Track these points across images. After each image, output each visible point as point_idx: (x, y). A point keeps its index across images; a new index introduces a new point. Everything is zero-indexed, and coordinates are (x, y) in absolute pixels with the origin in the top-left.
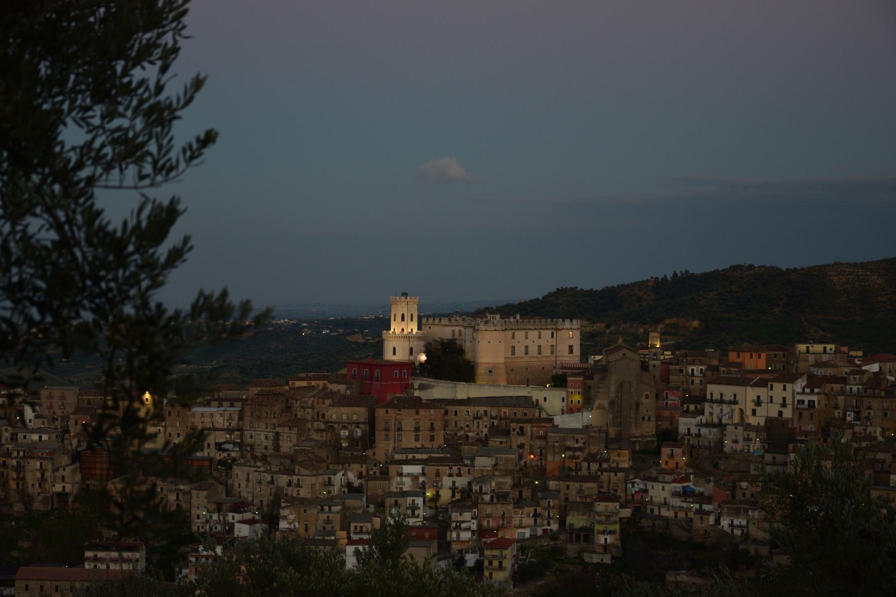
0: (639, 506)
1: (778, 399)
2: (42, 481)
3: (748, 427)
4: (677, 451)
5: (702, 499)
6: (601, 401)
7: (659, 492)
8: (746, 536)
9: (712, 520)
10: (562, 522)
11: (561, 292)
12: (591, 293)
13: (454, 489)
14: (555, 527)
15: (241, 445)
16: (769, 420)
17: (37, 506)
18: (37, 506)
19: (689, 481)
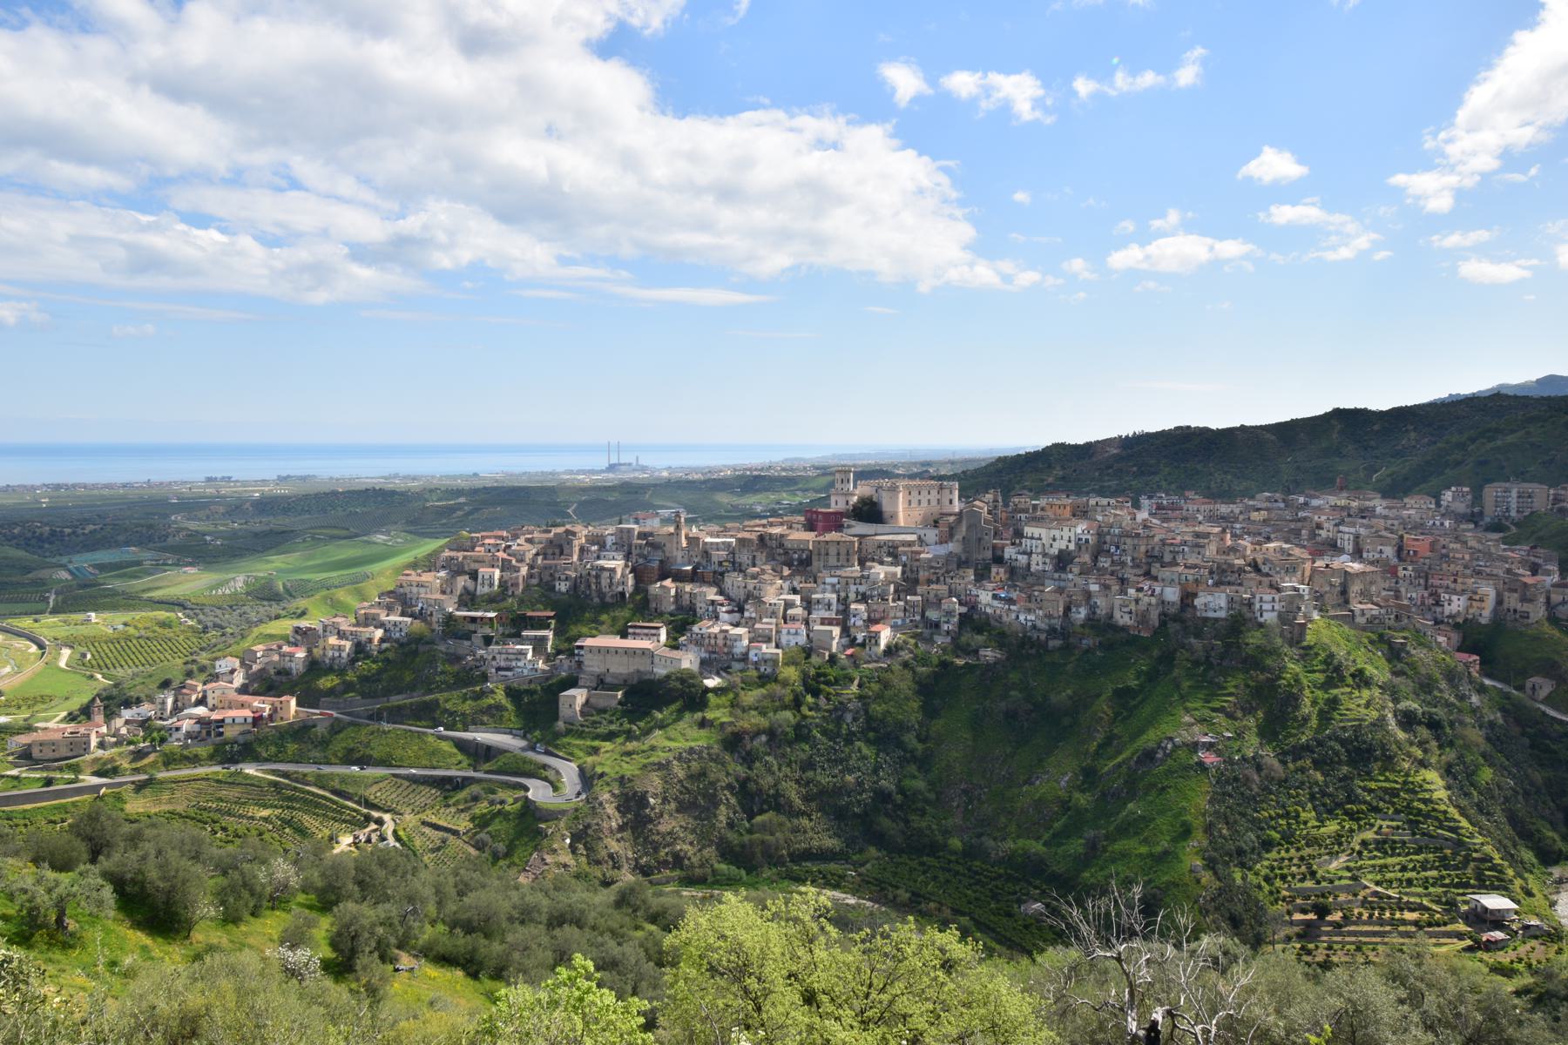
0: (973, 606)
1: (1066, 538)
2: (611, 584)
3: (1045, 555)
4: (1002, 570)
5: (1010, 601)
6: (959, 537)
7: (985, 597)
8: (1034, 627)
9: (1013, 616)
10: (923, 615)
11: (1056, 446)
12: (1076, 447)
13: (857, 593)
14: (918, 618)
15: (734, 563)
16: (1061, 551)
17: (608, 599)
18: (608, 599)
19: (547, 627)
